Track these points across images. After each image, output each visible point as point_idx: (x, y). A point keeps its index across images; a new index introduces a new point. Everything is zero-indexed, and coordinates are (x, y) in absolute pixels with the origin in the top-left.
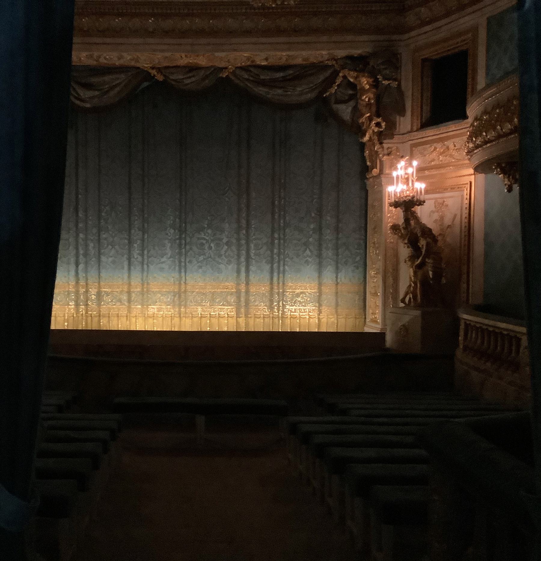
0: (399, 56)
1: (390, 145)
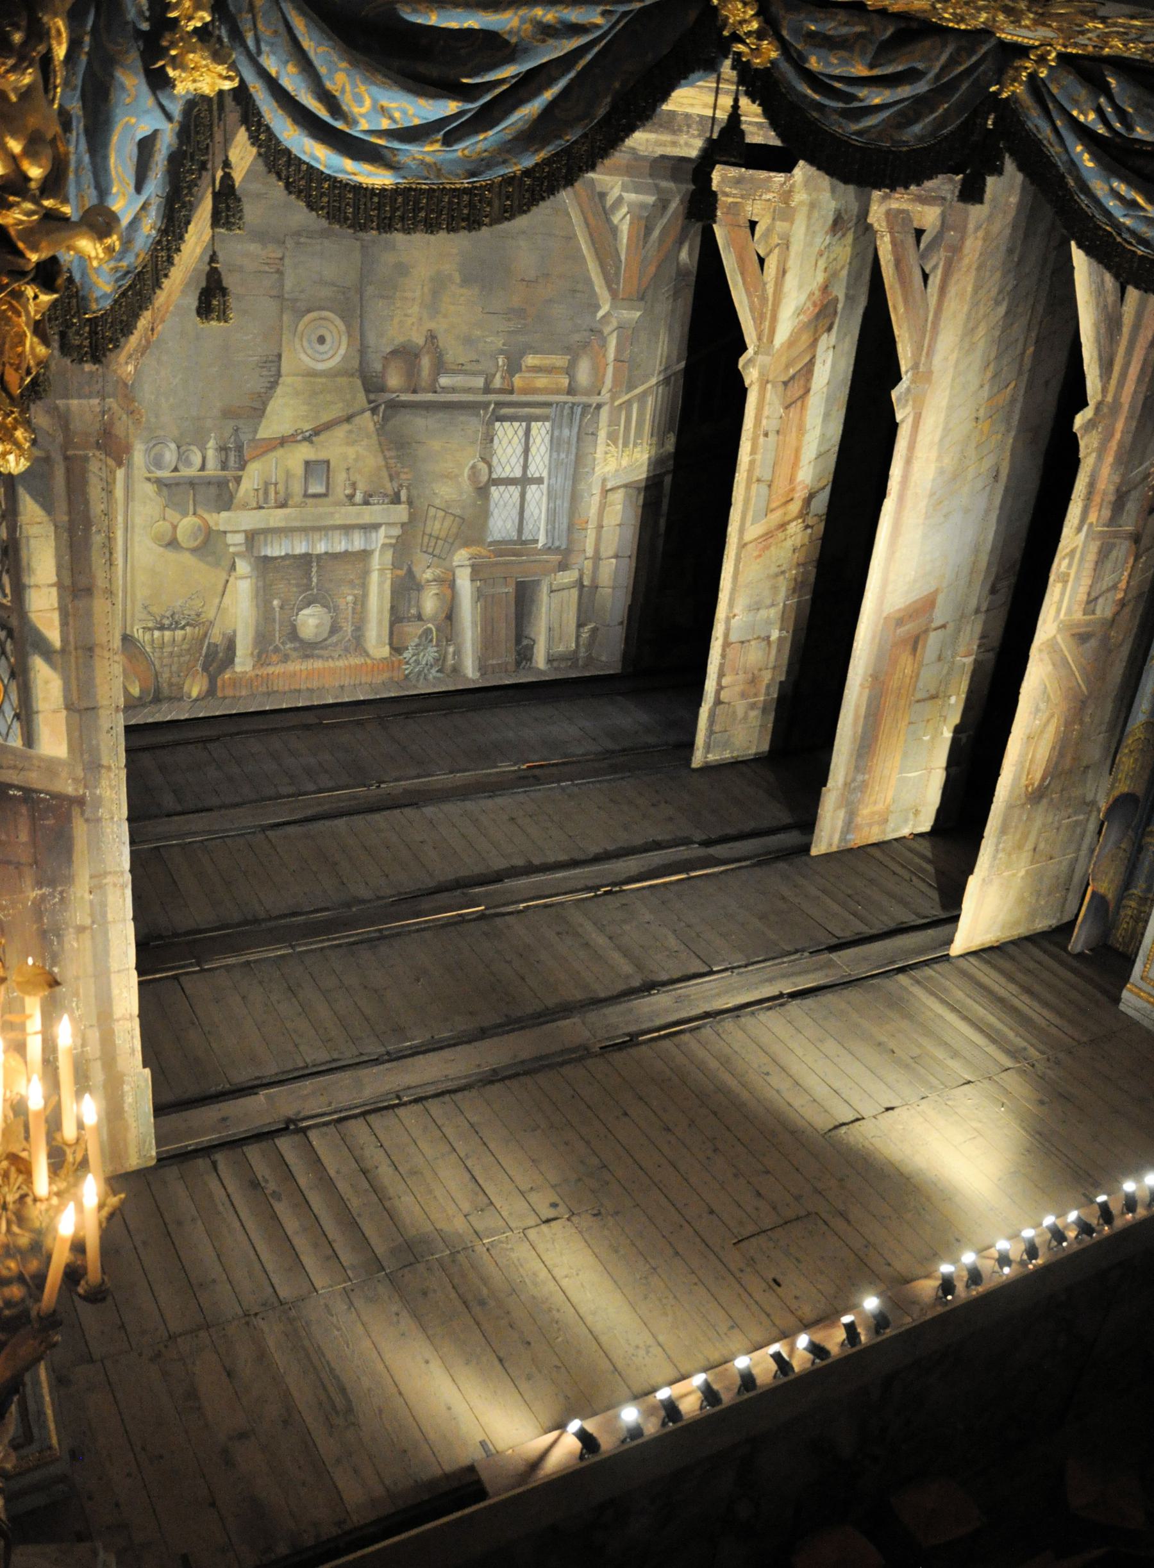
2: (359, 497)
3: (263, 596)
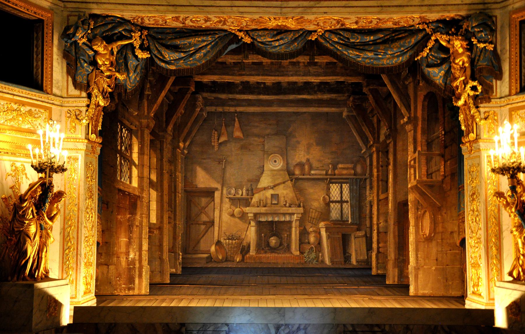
0: (494, 19)
1: (487, 109)
2: (287, 205)
3: (259, 232)
